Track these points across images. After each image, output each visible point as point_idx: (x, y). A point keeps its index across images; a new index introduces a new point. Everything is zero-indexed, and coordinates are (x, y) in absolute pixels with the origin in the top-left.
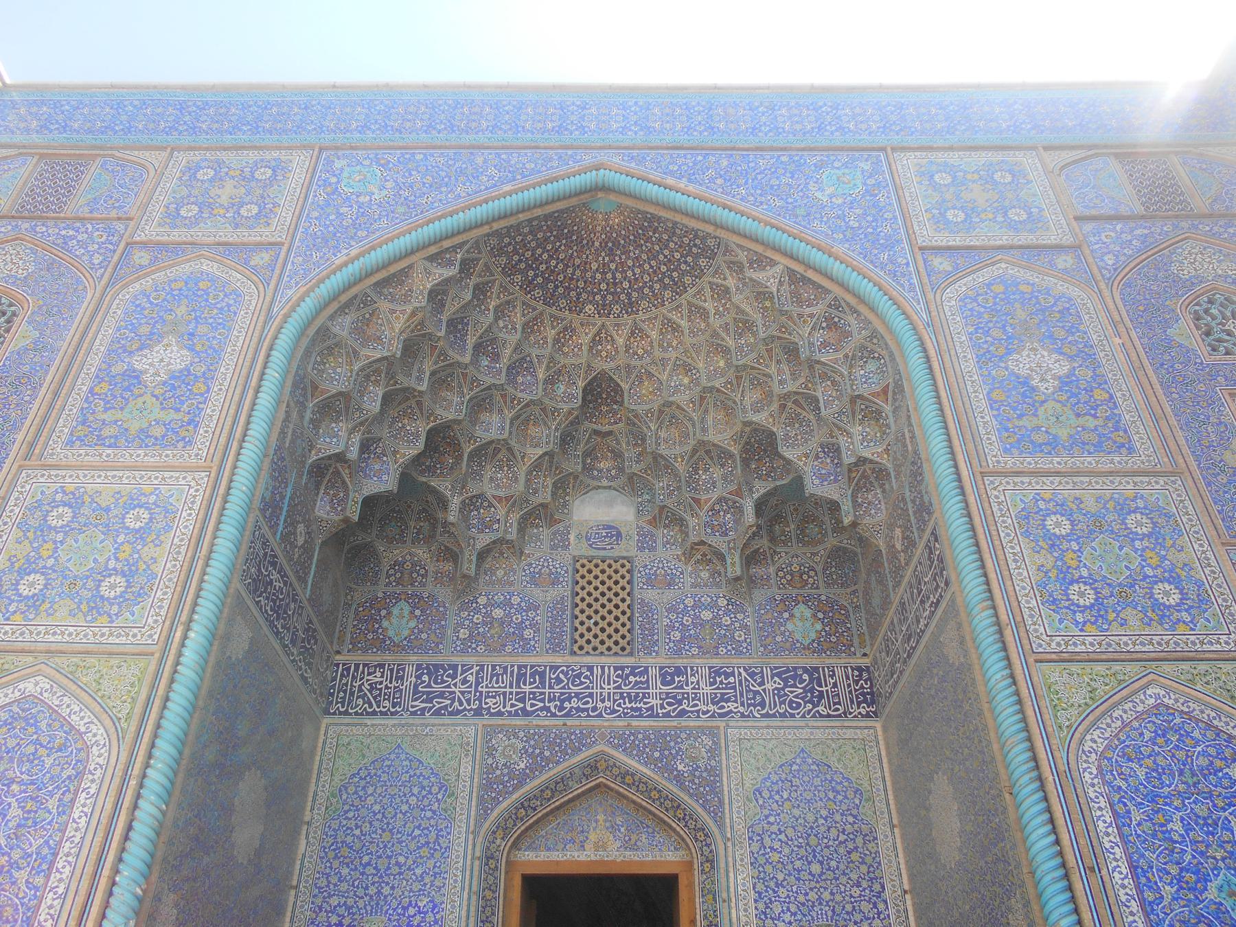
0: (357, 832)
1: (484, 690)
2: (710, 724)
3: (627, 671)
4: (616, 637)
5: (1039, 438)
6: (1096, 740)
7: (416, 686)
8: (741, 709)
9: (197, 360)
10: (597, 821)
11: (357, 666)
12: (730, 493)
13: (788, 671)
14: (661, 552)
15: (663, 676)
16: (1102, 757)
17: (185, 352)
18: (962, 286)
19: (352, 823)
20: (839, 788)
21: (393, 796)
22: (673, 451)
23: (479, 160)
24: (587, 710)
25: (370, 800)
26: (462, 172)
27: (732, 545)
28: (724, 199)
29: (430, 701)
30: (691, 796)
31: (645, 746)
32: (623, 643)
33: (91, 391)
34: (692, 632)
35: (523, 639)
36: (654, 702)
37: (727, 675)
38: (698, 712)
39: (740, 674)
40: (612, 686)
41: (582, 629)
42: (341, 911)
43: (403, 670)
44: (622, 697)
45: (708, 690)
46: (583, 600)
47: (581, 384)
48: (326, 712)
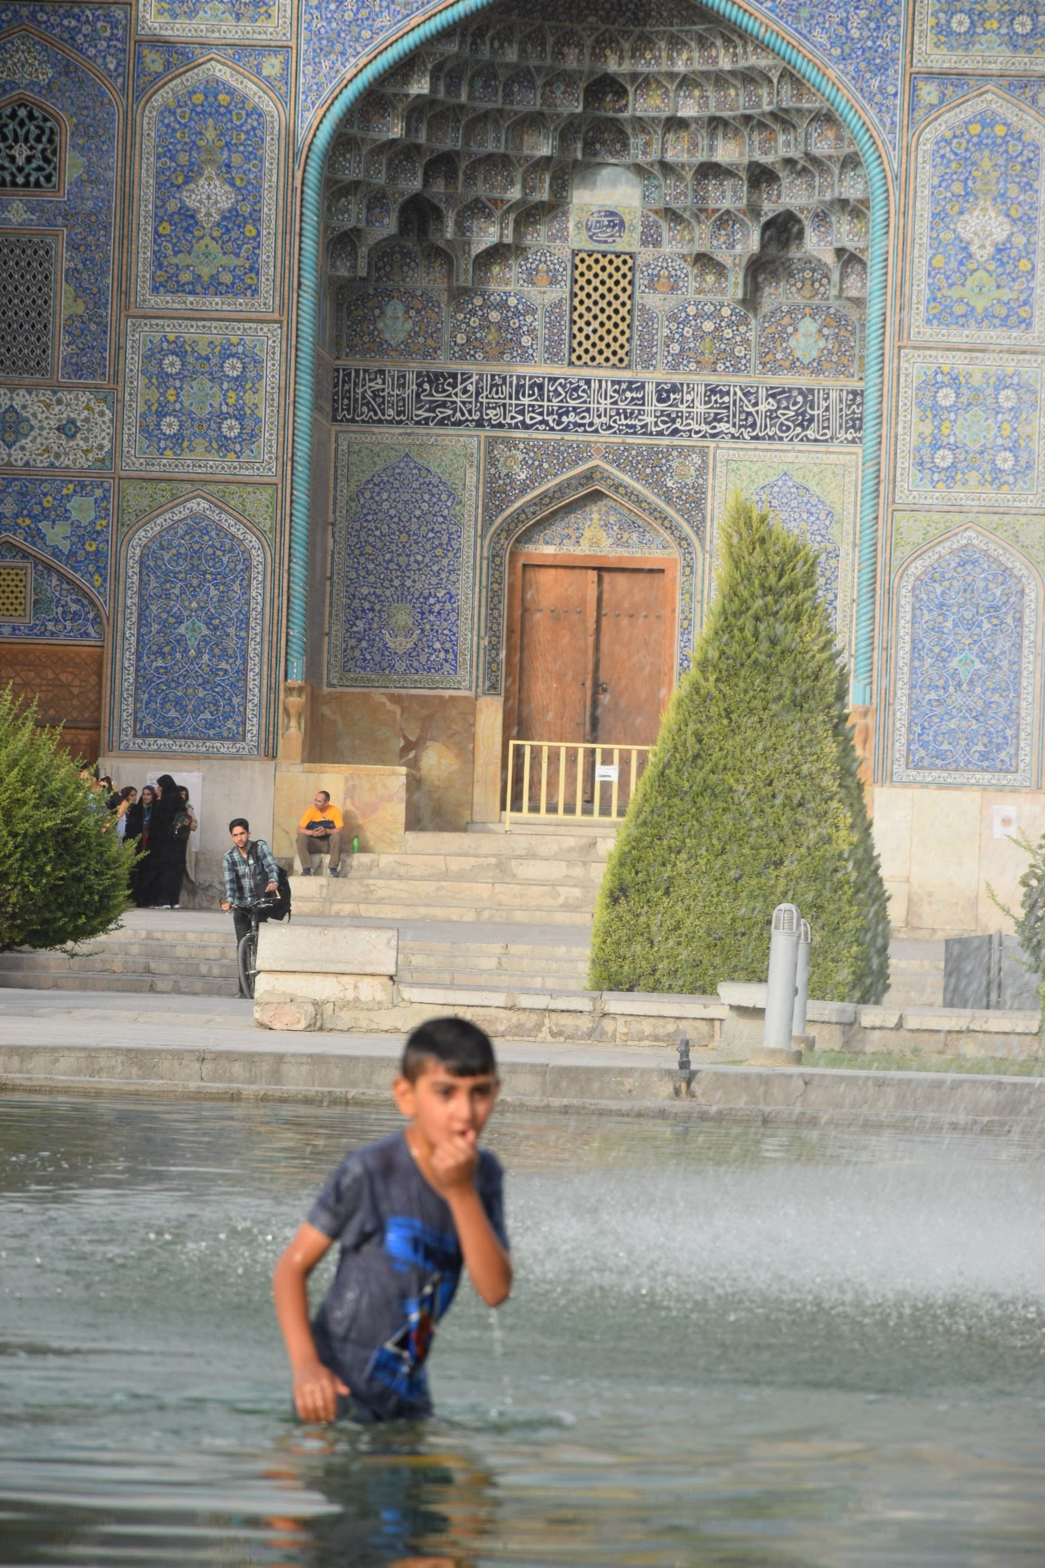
0: (378, 533)
1: (485, 401)
2: (700, 444)
3: (624, 386)
5: (959, 309)
6: (917, 568)
7: (418, 395)
8: (732, 430)
9: (240, 198)
10: (591, 520)
11: (357, 371)
12: (739, 210)
13: (783, 392)
14: (667, 249)
15: (659, 392)
16: (918, 579)
17: (227, 188)
18: (941, 127)
19: (372, 525)
20: (813, 510)
21: (406, 502)
22: (681, 159)
24: (583, 425)
25: (386, 505)
27: (737, 261)
30: (678, 511)
31: (638, 463)
32: (621, 353)
33: (156, 232)
34: (692, 345)
35: (521, 347)
36: (649, 419)
37: (723, 394)
38: (690, 431)
39: (735, 394)
40: (609, 401)
41: (580, 337)
42: (373, 598)
43: (404, 377)
44: (618, 414)
45: (700, 408)
46: (581, 302)
47: (583, 85)
48: (334, 419)
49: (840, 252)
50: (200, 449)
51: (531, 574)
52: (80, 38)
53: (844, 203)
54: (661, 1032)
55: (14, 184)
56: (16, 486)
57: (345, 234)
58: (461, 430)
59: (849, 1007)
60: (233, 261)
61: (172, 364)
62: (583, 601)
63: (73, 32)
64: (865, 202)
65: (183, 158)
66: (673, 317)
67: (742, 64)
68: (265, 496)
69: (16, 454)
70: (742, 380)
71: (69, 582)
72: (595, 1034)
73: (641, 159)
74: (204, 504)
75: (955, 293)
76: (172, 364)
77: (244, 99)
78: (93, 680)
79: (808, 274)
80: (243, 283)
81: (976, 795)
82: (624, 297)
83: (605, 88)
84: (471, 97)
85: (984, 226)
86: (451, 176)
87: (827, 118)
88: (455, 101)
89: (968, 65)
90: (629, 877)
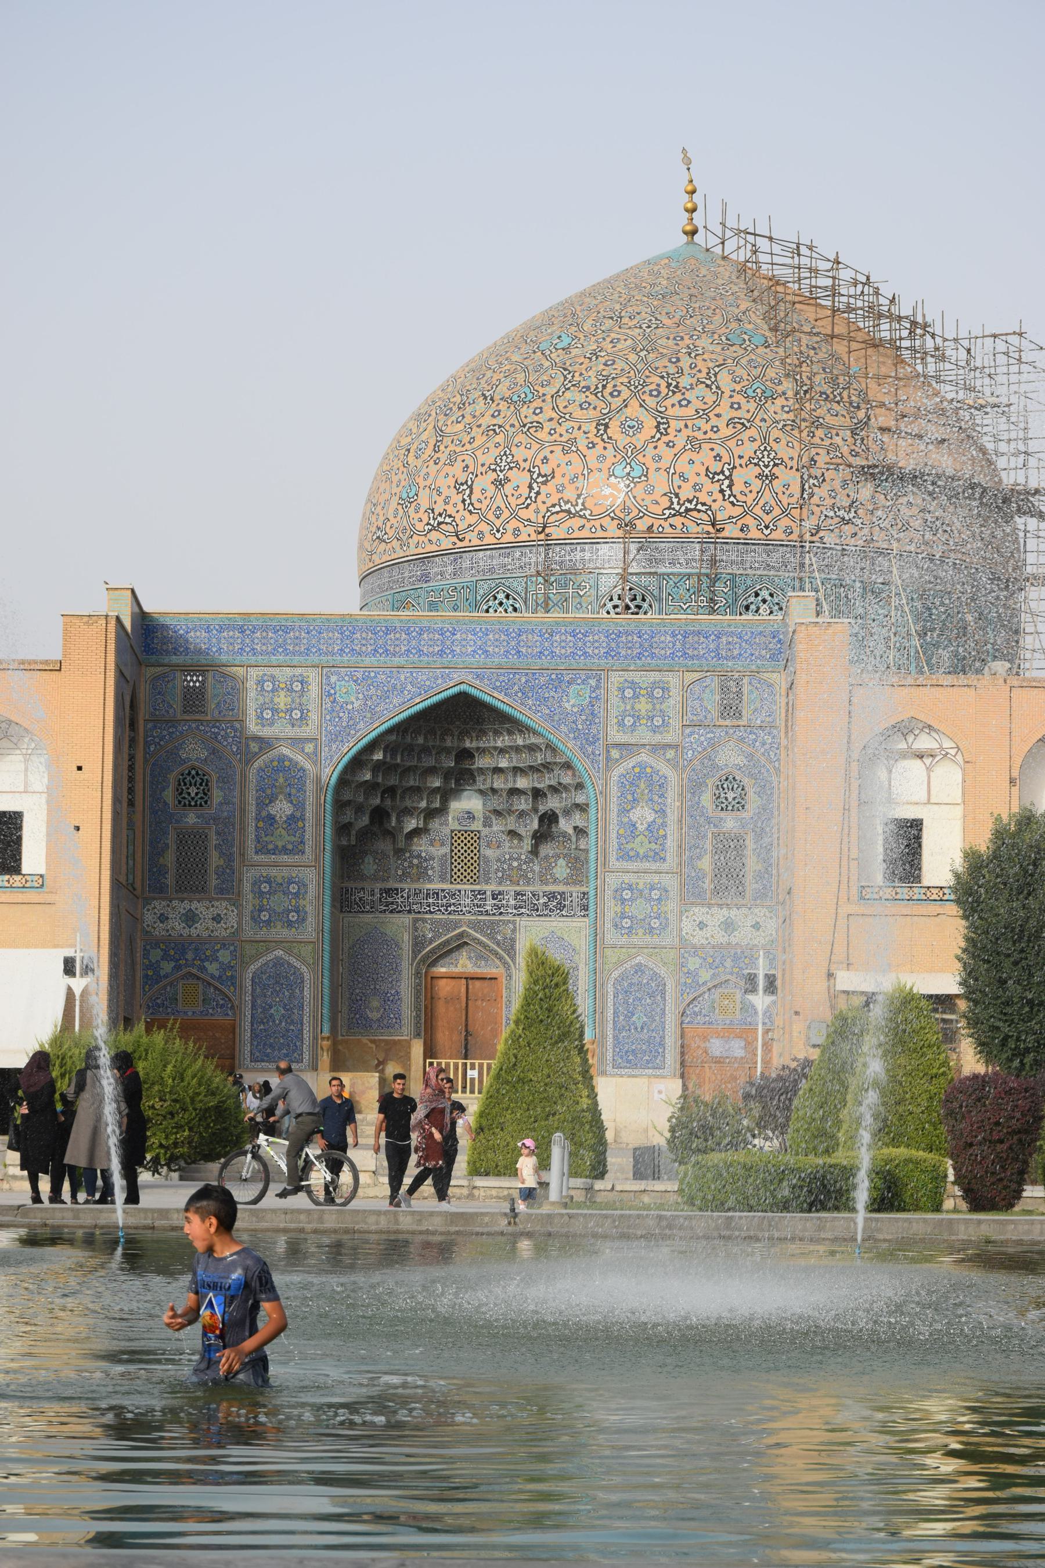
4: (472, 874)
5: (631, 854)
6: (616, 974)
14: (495, 828)
23: (403, 678)
26: (394, 687)
28: (522, 708)
29: (387, 906)
32: (475, 877)
36: (489, 908)
37: (523, 895)
41: (456, 870)
45: (512, 902)
47: (454, 753)
49: (575, 828)
50: (279, 927)
51: (435, 981)
52: (220, 737)
53: (577, 806)
54: (501, 1195)
55: (190, 805)
56: (193, 946)
57: (345, 825)
58: (401, 915)
59: (589, 1180)
60: (293, 839)
61: (265, 887)
62: (460, 991)
63: (216, 734)
64: (587, 805)
65: (269, 792)
66: (499, 860)
67: (528, 742)
68: (310, 947)
69: (193, 930)
70: (531, 888)
71: (219, 990)
72: (471, 1196)
73: (482, 787)
74: (281, 952)
75: (629, 846)
76: (265, 887)
77: (297, 763)
78: (231, 1036)
79: (561, 839)
80: (297, 849)
81: (645, 1080)
82: (475, 851)
83: (465, 755)
84: (402, 760)
85: (643, 815)
86: (393, 797)
87: (568, 766)
88: (394, 762)
89: (633, 741)
90: (484, 1123)
